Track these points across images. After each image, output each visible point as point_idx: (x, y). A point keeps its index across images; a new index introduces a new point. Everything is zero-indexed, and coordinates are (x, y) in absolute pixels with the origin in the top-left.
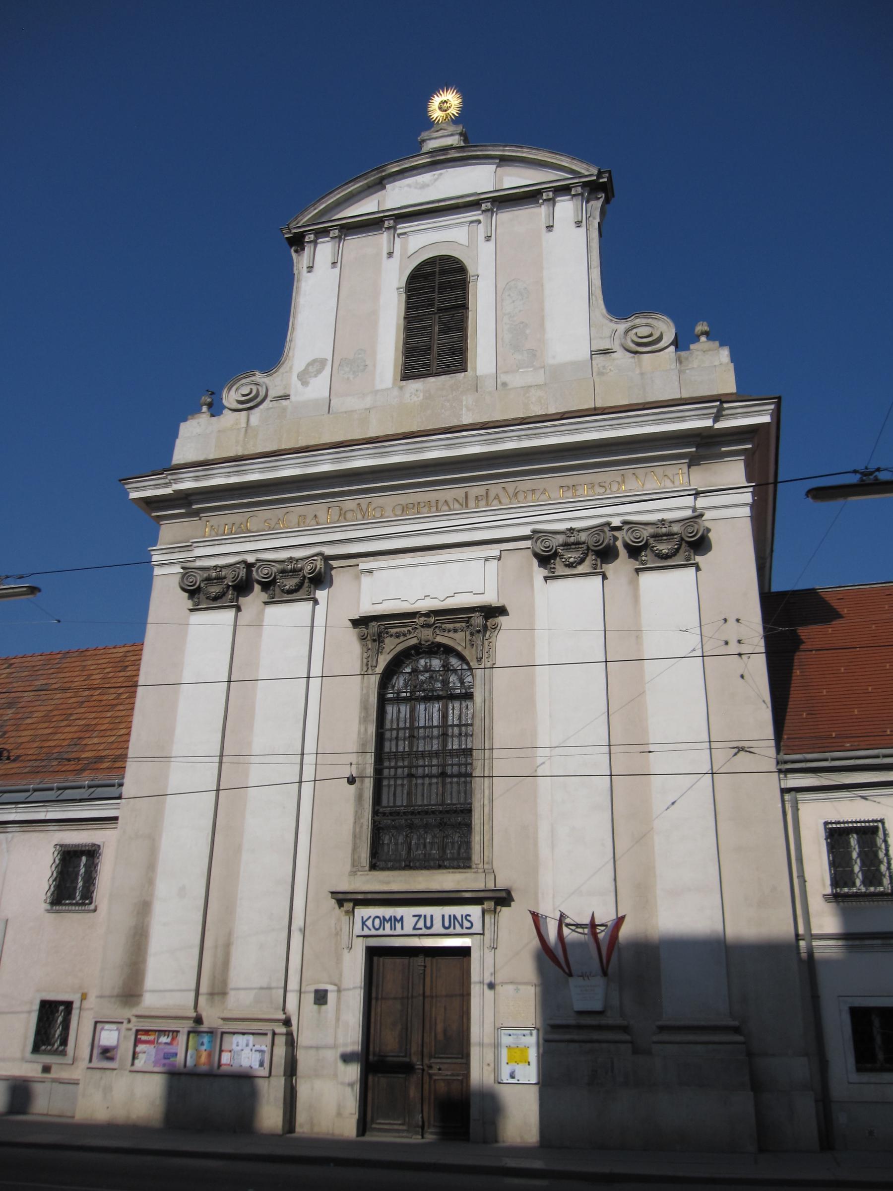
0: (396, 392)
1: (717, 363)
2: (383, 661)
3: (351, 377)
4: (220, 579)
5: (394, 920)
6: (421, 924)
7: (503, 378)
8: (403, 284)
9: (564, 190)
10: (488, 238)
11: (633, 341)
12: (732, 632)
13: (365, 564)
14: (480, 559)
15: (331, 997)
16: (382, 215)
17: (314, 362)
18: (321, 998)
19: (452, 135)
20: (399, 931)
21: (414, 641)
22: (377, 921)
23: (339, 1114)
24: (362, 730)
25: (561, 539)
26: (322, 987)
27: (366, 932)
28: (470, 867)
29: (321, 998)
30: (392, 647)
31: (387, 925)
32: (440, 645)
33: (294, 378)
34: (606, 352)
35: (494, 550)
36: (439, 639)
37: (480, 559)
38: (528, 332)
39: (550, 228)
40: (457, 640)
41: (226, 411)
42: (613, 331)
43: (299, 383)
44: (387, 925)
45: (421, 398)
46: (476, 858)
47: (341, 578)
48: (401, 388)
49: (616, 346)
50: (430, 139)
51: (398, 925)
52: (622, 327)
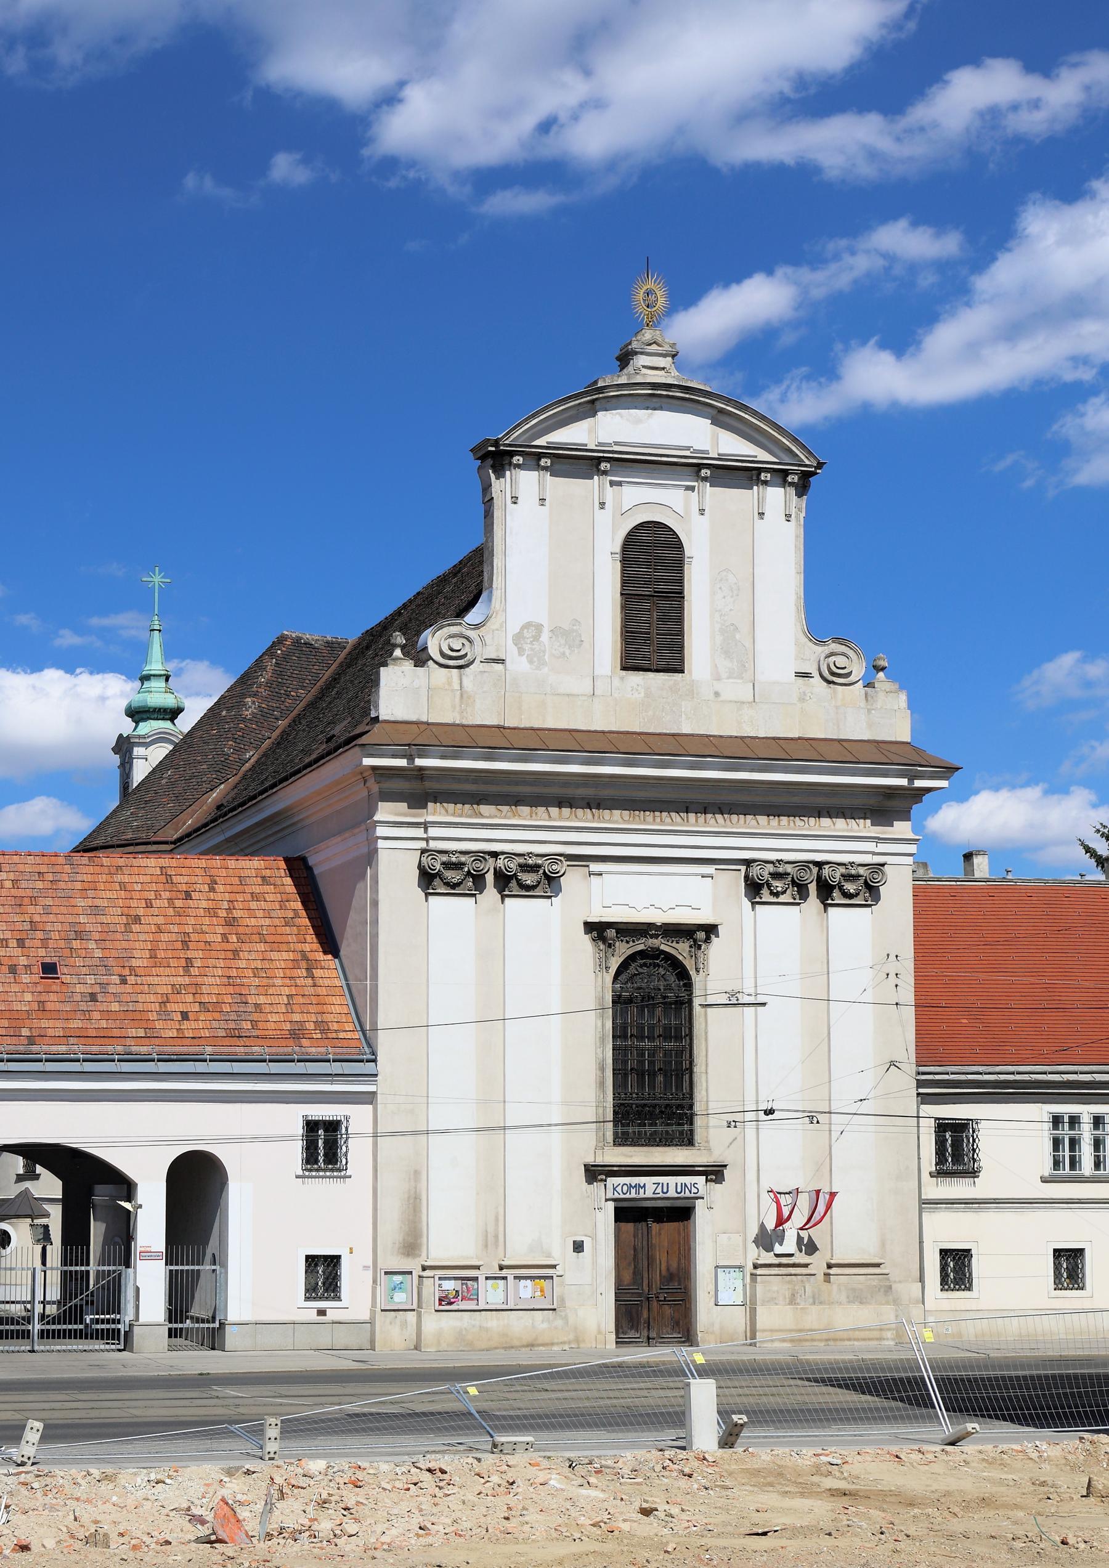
0: (616, 682)
1: (896, 707)
2: (615, 963)
3: (567, 652)
4: (458, 866)
5: (638, 1187)
6: (659, 1190)
7: (718, 686)
8: (618, 548)
9: (781, 476)
10: (702, 512)
11: (828, 666)
12: (892, 967)
13: (595, 867)
14: (697, 875)
15: (587, 1246)
16: (601, 455)
17: (527, 626)
18: (578, 1247)
19: (664, 356)
20: (642, 1195)
21: (641, 947)
22: (625, 1188)
23: (599, 1332)
24: (599, 1024)
25: (770, 868)
26: (578, 1239)
27: (616, 1196)
28: (693, 1145)
29: (578, 1247)
30: (624, 949)
31: (633, 1191)
32: (663, 952)
33: (510, 642)
34: (806, 675)
35: (710, 869)
36: (663, 947)
37: (697, 875)
38: (738, 636)
39: (761, 514)
40: (681, 949)
41: (430, 663)
42: (813, 655)
43: (515, 649)
44: (633, 1191)
45: (642, 695)
46: (698, 1137)
47: (572, 879)
48: (622, 678)
49: (816, 674)
50: (642, 353)
51: (642, 1191)
52: (821, 651)
